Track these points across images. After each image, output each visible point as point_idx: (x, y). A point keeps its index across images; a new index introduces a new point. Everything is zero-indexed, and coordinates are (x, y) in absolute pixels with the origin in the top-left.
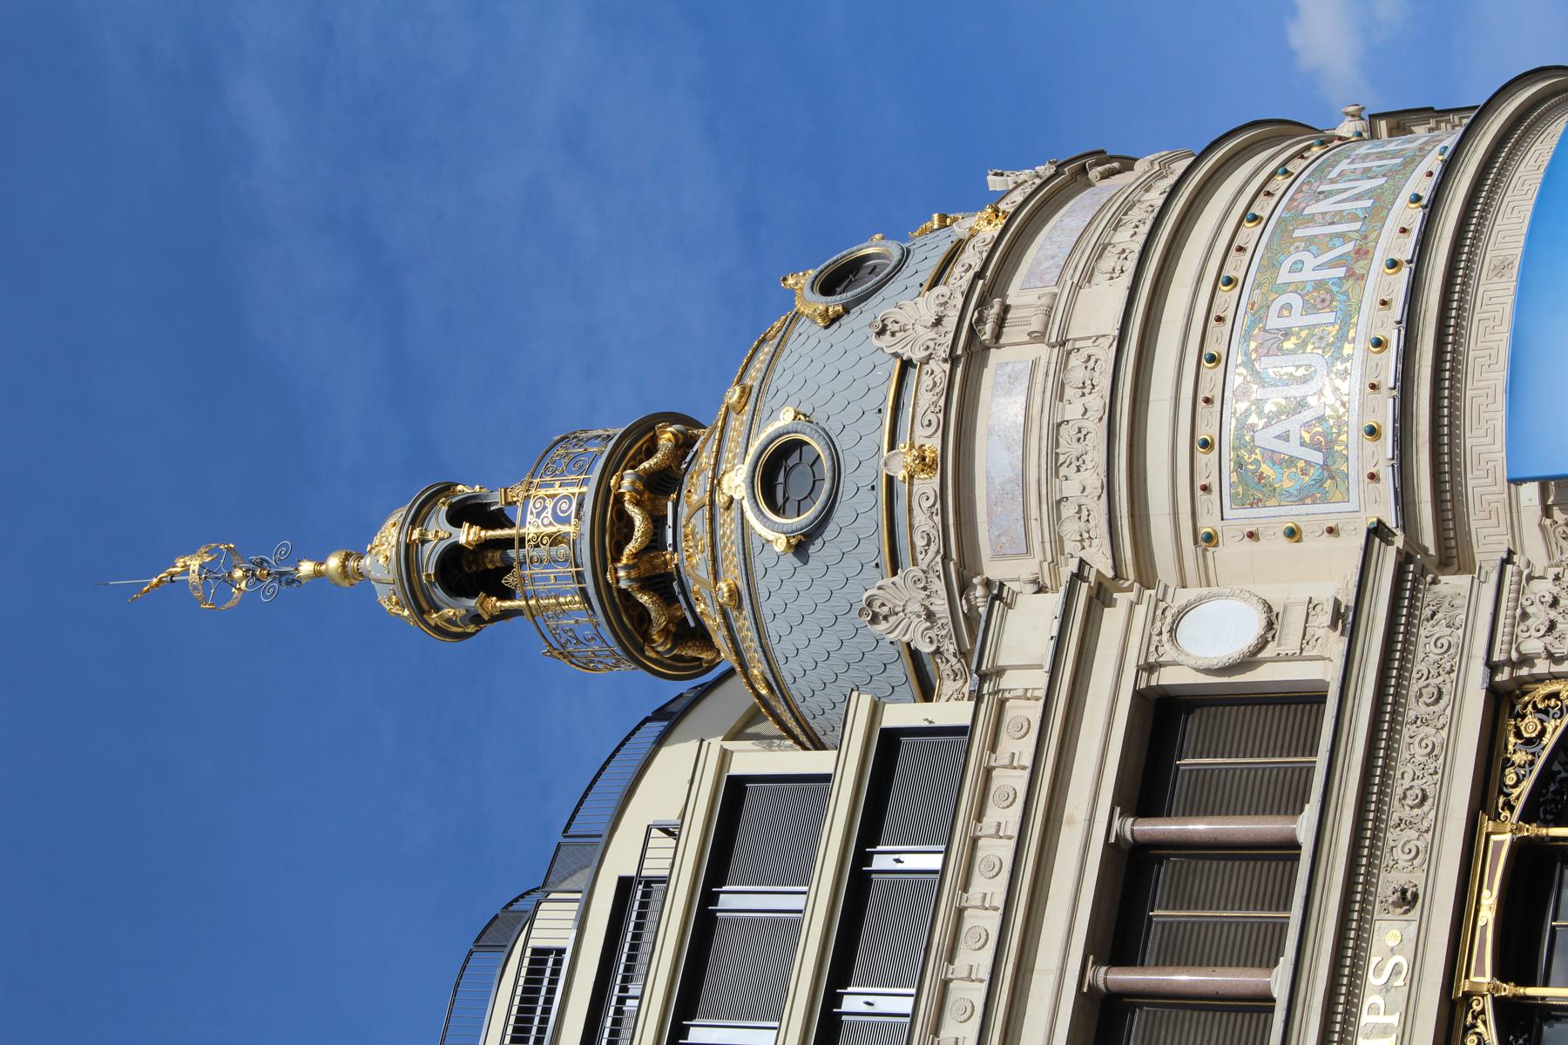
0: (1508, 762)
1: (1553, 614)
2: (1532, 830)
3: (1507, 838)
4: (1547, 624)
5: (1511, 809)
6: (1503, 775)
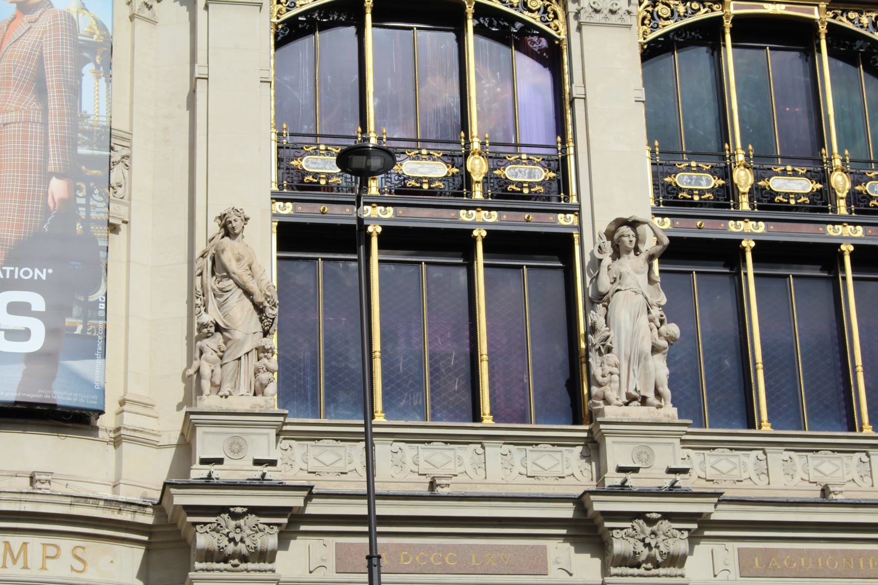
0: (861, 13)
1: (606, 12)
2: (823, 30)
3: (816, 16)
4: (598, 8)
5: (834, 17)
6: (854, 11)
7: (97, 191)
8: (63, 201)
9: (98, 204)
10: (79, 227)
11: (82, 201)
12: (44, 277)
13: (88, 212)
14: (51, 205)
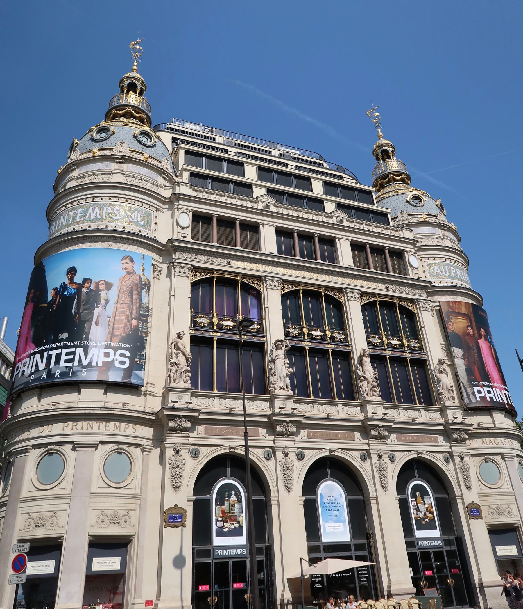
7: (144, 324)
8: (135, 326)
9: (145, 328)
10: (139, 333)
11: (141, 326)
12: (130, 347)
13: (142, 329)
14: (133, 327)
